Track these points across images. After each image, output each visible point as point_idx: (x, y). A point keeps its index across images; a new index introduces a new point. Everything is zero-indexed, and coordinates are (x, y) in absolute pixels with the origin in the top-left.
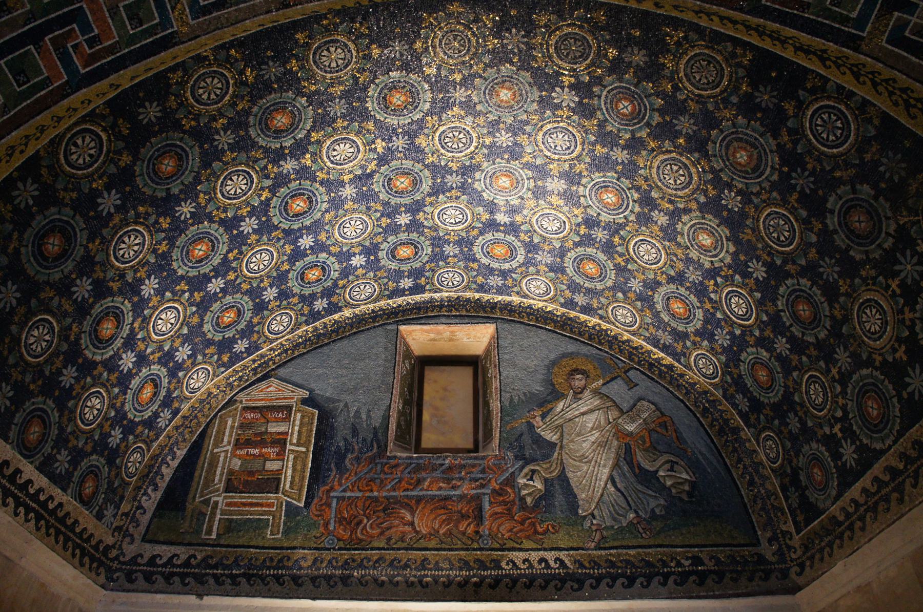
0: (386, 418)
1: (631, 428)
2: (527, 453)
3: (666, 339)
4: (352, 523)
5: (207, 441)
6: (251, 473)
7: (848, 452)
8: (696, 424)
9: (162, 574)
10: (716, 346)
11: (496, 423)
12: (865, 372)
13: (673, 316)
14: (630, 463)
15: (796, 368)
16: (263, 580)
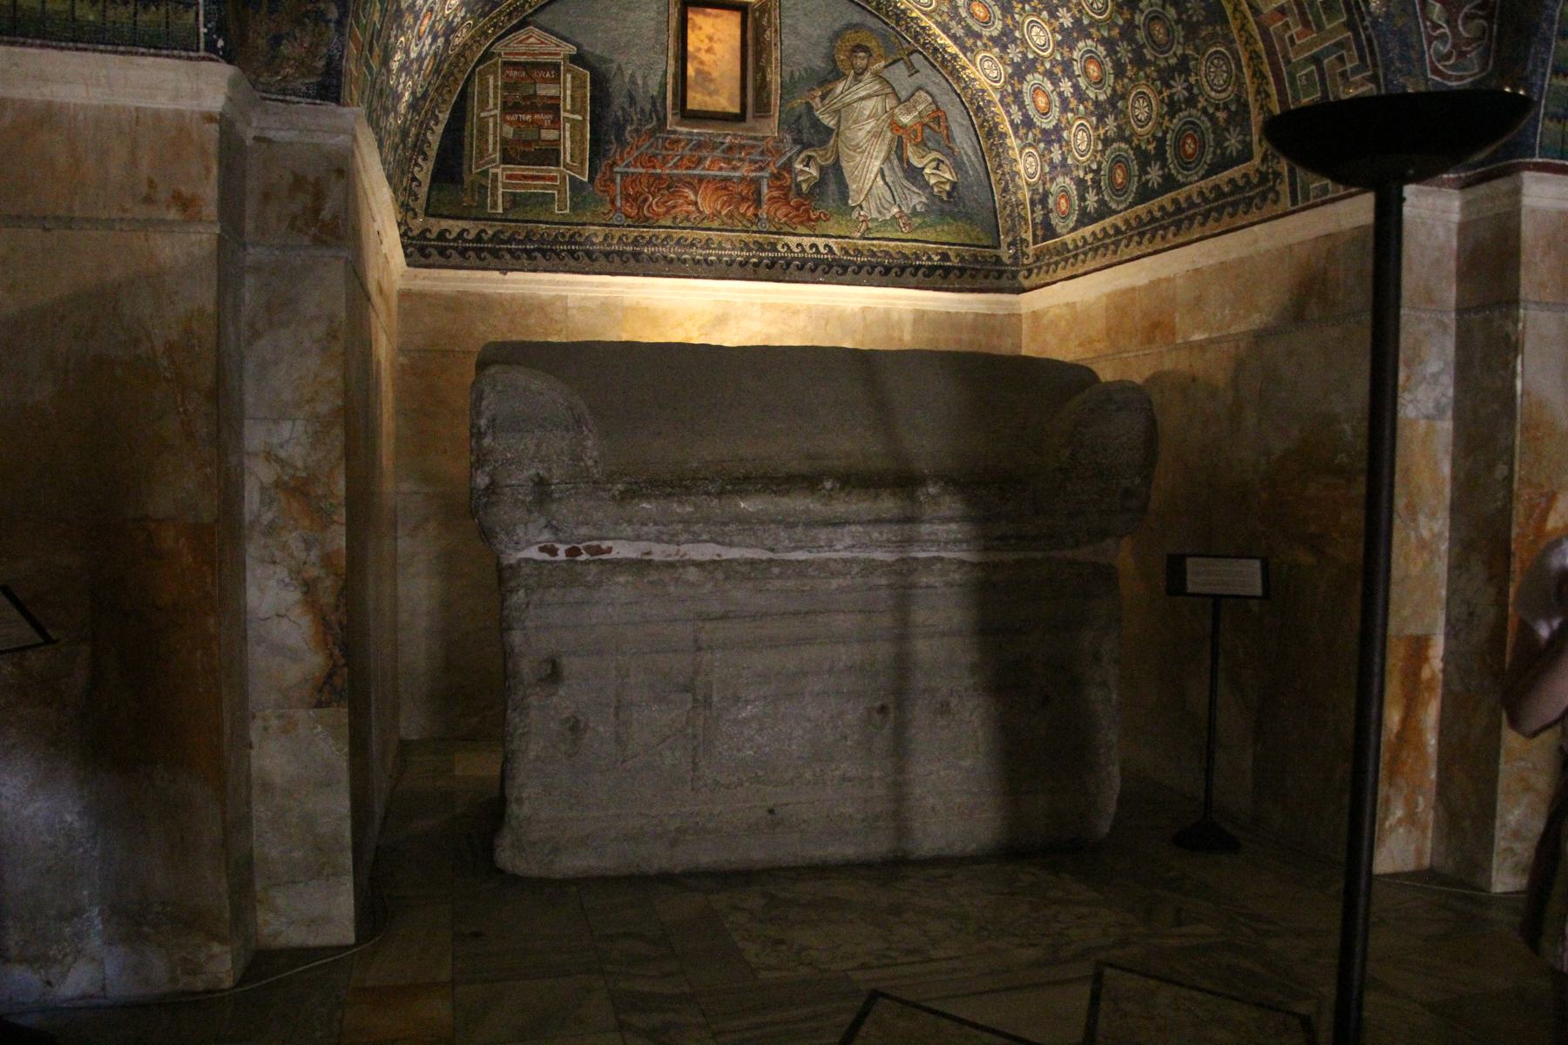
0: (663, 85)
1: (906, 119)
2: (805, 137)
3: (960, 33)
4: (636, 200)
5: (469, 102)
6: (527, 143)
7: (1092, 198)
8: (966, 122)
9: (456, 248)
10: (1007, 58)
11: (775, 100)
12: (1123, 145)
13: (972, 15)
14: (900, 159)
15: (1072, 110)
16: (558, 255)
